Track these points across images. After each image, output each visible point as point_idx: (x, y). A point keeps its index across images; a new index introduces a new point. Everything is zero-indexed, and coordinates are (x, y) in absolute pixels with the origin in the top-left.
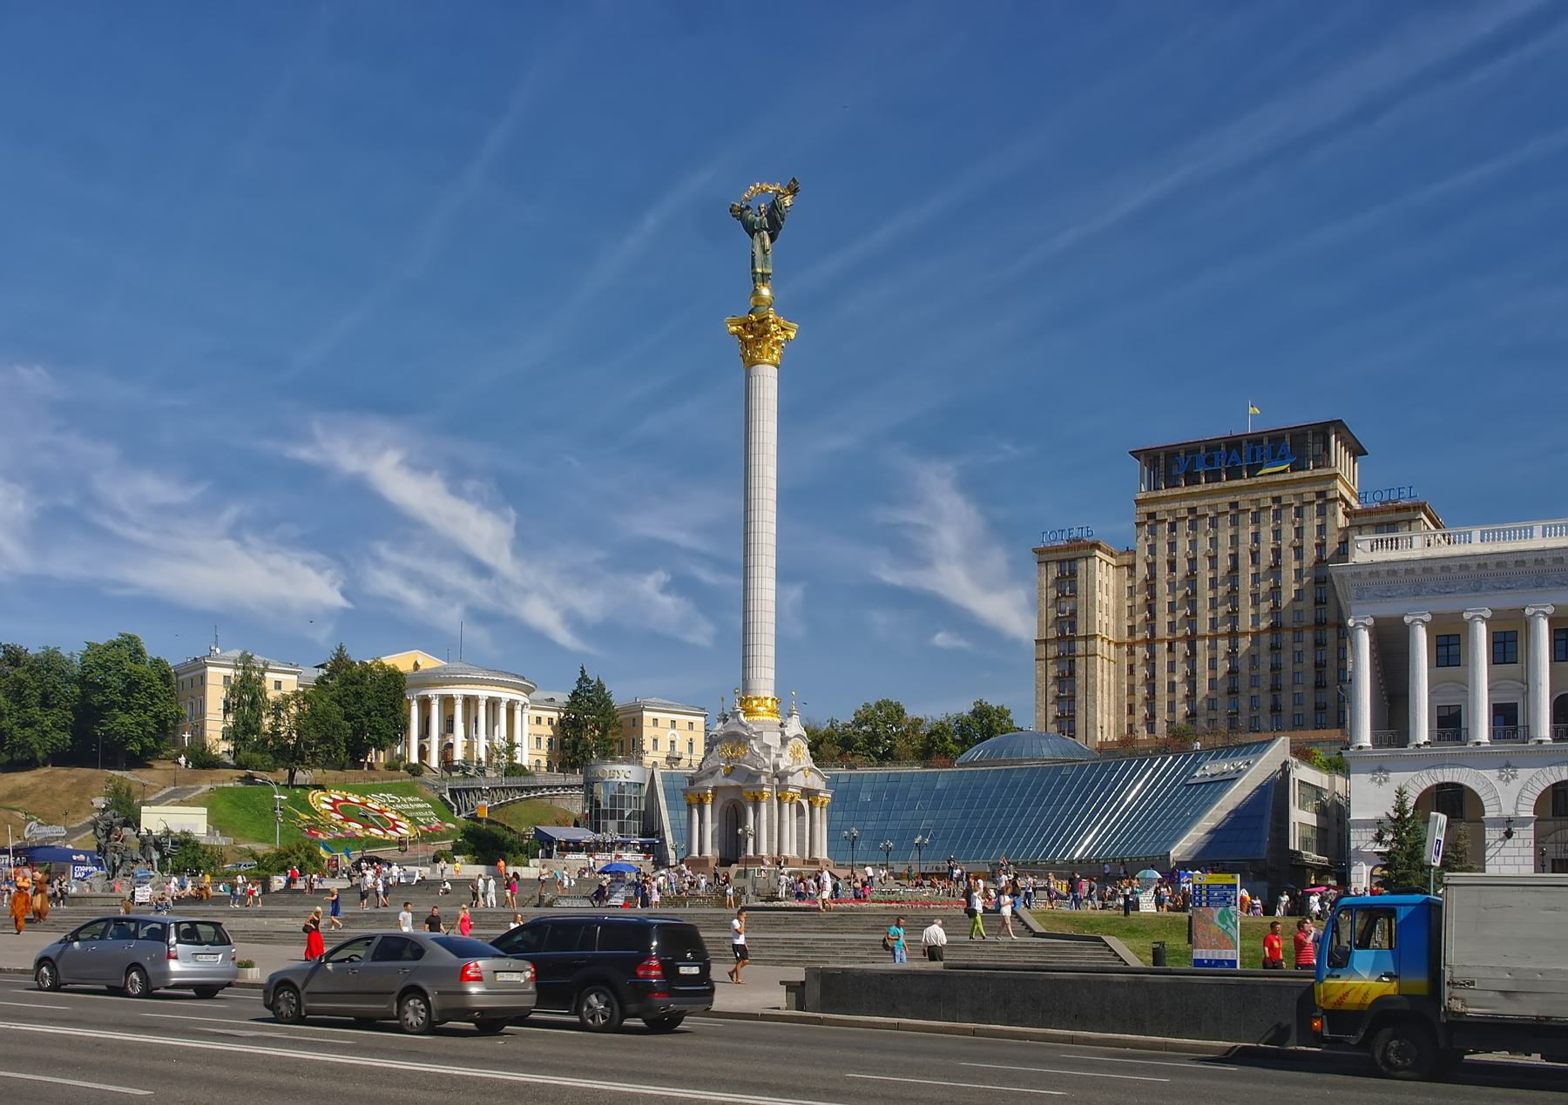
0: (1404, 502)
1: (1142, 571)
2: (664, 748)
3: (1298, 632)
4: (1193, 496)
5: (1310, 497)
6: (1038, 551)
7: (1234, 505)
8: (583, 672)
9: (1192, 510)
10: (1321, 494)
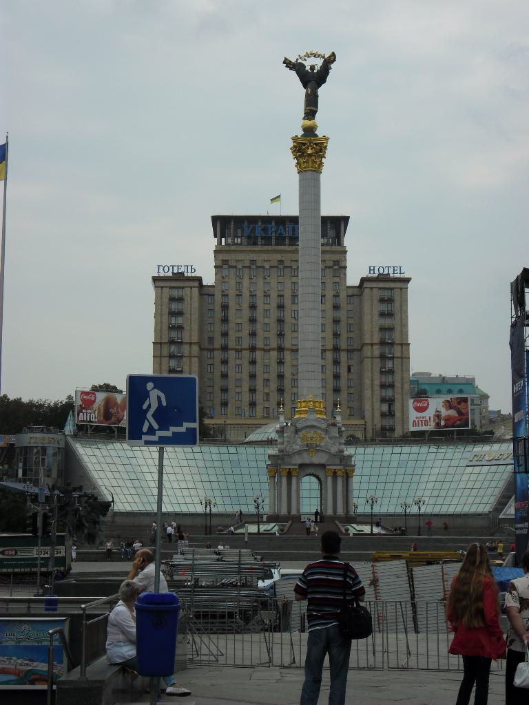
0: (398, 276)
1: (218, 297)
4: (254, 252)
6: (155, 279)
7: (281, 262)
9: (253, 262)
10: (336, 262)
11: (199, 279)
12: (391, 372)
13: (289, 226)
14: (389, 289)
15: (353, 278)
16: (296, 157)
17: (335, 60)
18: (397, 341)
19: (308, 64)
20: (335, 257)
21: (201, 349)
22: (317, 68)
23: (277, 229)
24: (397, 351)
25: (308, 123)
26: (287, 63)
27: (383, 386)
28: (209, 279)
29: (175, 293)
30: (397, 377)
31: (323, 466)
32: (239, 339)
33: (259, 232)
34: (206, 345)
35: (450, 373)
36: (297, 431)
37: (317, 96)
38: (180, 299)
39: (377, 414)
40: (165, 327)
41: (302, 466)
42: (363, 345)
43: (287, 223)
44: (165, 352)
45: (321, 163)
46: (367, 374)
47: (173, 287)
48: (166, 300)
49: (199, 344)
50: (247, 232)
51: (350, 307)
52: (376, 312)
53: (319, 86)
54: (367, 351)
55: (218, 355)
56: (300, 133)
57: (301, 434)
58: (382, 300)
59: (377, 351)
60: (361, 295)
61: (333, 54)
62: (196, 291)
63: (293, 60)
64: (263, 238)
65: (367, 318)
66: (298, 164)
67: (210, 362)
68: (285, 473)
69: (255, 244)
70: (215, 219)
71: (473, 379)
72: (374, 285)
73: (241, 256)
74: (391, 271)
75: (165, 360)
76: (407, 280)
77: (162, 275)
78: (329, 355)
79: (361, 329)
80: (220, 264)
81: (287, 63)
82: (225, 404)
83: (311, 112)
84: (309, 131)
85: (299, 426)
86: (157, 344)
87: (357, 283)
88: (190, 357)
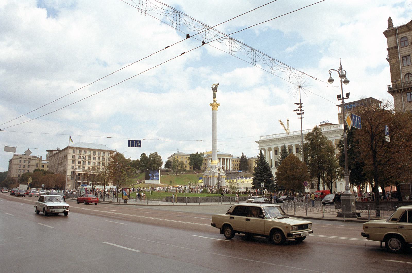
13: (356, 104)
17: (219, 84)
23: (353, 105)
33: (348, 107)
43: (356, 103)
56: (212, 102)
61: (218, 83)
77: (321, 124)
80: (340, 118)
83: (215, 97)
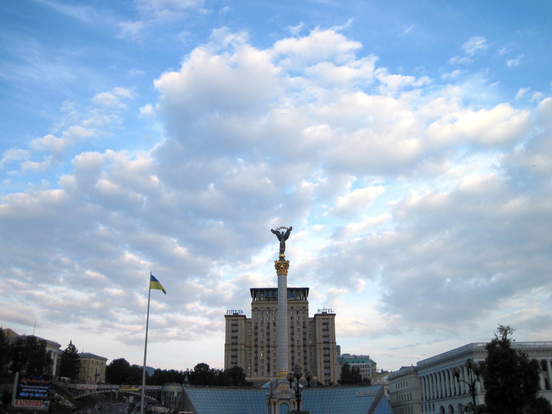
1: (253, 325)
2: (94, 372)
3: (299, 347)
4: (268, 303)
5: (301, 308)
6: (226, 316)
8: (71, 342)
9: (268, 308)
10: (304, 308)
11: (245, 316)
12: (329, 355)
14: (327, 319)
15: (311, 315)
16: (276, 269)
18: (331, 341)
19: (281, 231)
20: (304, 305)
21: (246, 347)
22: (285, 233)
24: (331, 346)
25: (282, 255)
26: (273, 231)
27: (325, 362)
28: (249, 316)
29: (235, 322)
30: (331, 357)
31: (289, 399)
32: (262, 342)
34: (248, 344)
35: (358, 354)
36: (277, 385)
37: (284, 244)
38: (237, 325)
39: (323, 374)
40: (230, 337)
41: (279, 399)
42: (316, 344)
44: (230, 348)
45: (287, 271)
46: (318, 356)
47: (234, 321)
48: (230, 325)
49: (245, 344)
50: (266, 295)
51: (310, 327)
52: (321, 329)
53: (286, 240)
54: (318, 346)
55: (253, 349)
56: (278, 259)
57: (279, 386)
58: (324, 324)
59: (322, 346)
60: (315, 321)
61: (291, 227)
62: (243, 321)
63: (275, 230)
64: (272, 298)
65: (318, 331)
66: (277, 272)
67: (250, 352)
68: (272, 403)
69: (269, 300)
70: (252, 290)
71: (368, 356)
72: (320, 317)
73: (263, 306)
74: (327, 311)
75: (230, 352)
76: (334, 315)
78: (302, 349)
79: (315, 337)
81: (273, 231)
82: (256, 371)
84: (282, 258)
85: (278, 382)
86: (226, 345)
87: (313, 316)
88: (241, 350)
